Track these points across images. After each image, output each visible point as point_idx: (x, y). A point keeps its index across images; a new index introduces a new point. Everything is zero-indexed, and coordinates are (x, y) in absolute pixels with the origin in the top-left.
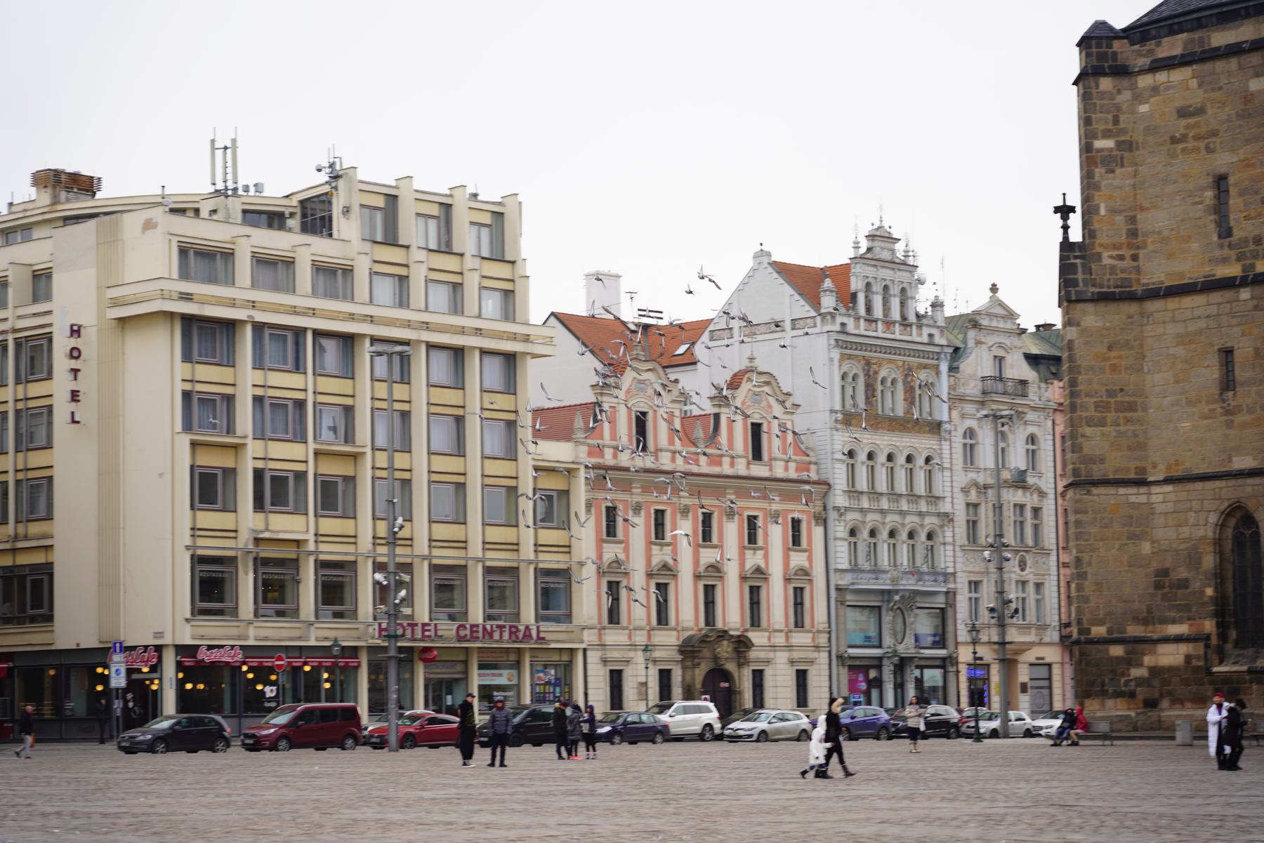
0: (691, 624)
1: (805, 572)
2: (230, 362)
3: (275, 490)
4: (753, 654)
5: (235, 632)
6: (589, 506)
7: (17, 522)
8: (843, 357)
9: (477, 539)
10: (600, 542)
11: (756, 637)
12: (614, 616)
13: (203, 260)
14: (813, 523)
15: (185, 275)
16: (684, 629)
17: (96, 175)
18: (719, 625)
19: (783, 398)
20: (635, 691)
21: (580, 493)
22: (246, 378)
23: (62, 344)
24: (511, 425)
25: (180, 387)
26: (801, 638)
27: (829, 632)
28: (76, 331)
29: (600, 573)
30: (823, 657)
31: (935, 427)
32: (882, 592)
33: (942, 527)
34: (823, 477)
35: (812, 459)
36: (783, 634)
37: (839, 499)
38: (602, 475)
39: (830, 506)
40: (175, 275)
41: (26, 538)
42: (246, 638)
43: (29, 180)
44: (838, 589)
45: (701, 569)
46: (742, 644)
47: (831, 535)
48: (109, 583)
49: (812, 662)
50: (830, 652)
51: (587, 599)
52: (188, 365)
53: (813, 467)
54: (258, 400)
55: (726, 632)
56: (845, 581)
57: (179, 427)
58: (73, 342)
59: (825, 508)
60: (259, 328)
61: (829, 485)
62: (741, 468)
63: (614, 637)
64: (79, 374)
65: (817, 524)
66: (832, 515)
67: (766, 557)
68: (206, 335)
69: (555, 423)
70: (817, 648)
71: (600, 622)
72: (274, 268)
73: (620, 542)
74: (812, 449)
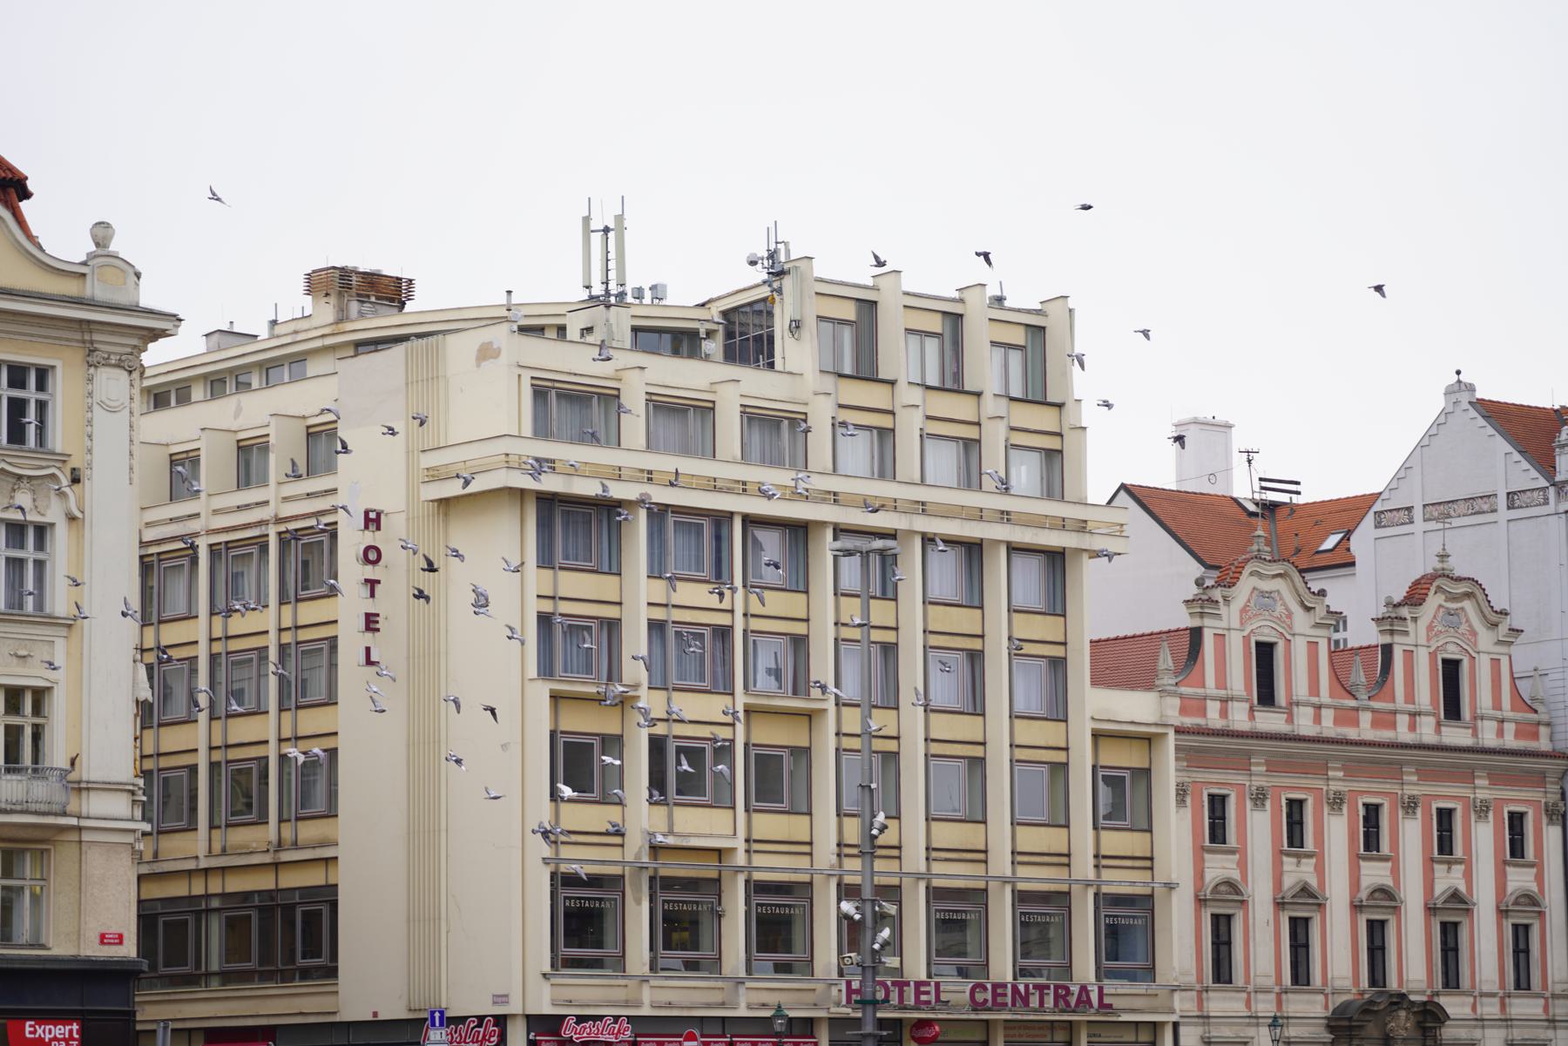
0: (1348, 983)
2: (614, 568)
3: (681, 771)
5: (620, 994)
6: (1182, 792)
7: (281, 821)
9: (1003, 847)
10: (1200, 852)
11: (1454, 1006)
12: (1222, 971)
13: (569, 406)
14: (1545, 820)
15: (542, 430)
17: (405, 275)
18: (1393, 984)
19: (1495, 617)
21: (1168, 770)
22: (638, 592)
23: (351, 540)
24: (1058, 665)
25: (534, 607)
28: (373, 520)
29: (1201, 902)
35: (1544, 717)
36: (1496, 1000)
38: (1206, 746)
40: (528, 430)
41: (295, 845)
42: (638, 1005)
43: (301, 285)
45: (1363, 895)
48: (424, 920)
51: (1180, 942)
52: (548, 573)
53: (1543, 730)
54: (656, 627)
55: (1403, 996)
57: (532, 671)
58: (369, 538)
60: (659, 513)
62: (1427, 731)
63: (1222, 1003)
64: (378, 588)
65: (1551, 822)
67: (1468, 875)
68: (575, 524)
69: (1122, 661)
71: (1200, 979)
72: (682, 417)
73: (1232, 852)
74: (1542, 702)
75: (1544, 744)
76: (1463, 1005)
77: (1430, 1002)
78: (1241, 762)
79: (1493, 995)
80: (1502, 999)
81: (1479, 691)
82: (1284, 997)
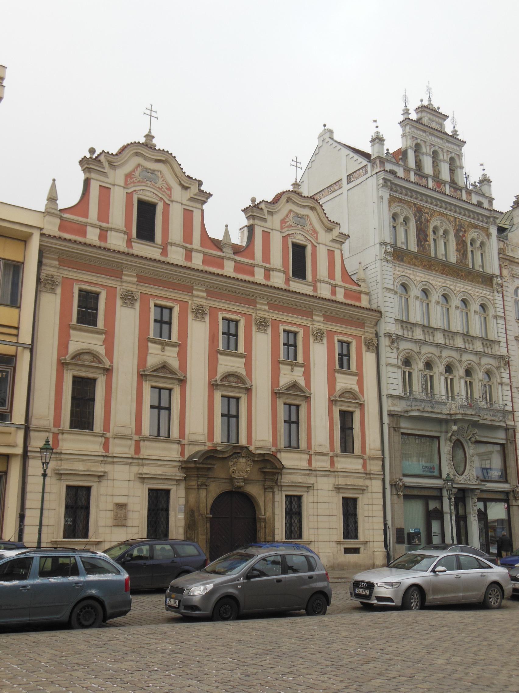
0: (203, 438)
4: (286, 479)
8: (392, 200)
11: (288, 459)
14: (364, 348)
16: (193, 443)
20: (110, 515)
26: (346, 463)
27: (383, 460)
30: (376, 486)
31: (487, 280)
32: (440, 421)
33: (498, 368)
34: (374, 307)
35: (365, 290)
36: (327, 458)
37: (388, 326)
39: (381, 334)
44: (391, 415)
46: (268, 467)
49: (363, 490)
50: (384, 480)
53: (363, 296)
56: (399, 407)
59: (377, 335)
61: (380, 312)
62: (278, 280)
65: (368, 349)
66: (384, 342)
67: (307, 375)
70: (368, 475)
74: (364, 281)
75: (364, 303)
76: (301, 459)
77: (274, 456)
78: (116, 272)
79: (325, 454)
80: (332, 458)
81: (319, 263)
82: (142, 443)
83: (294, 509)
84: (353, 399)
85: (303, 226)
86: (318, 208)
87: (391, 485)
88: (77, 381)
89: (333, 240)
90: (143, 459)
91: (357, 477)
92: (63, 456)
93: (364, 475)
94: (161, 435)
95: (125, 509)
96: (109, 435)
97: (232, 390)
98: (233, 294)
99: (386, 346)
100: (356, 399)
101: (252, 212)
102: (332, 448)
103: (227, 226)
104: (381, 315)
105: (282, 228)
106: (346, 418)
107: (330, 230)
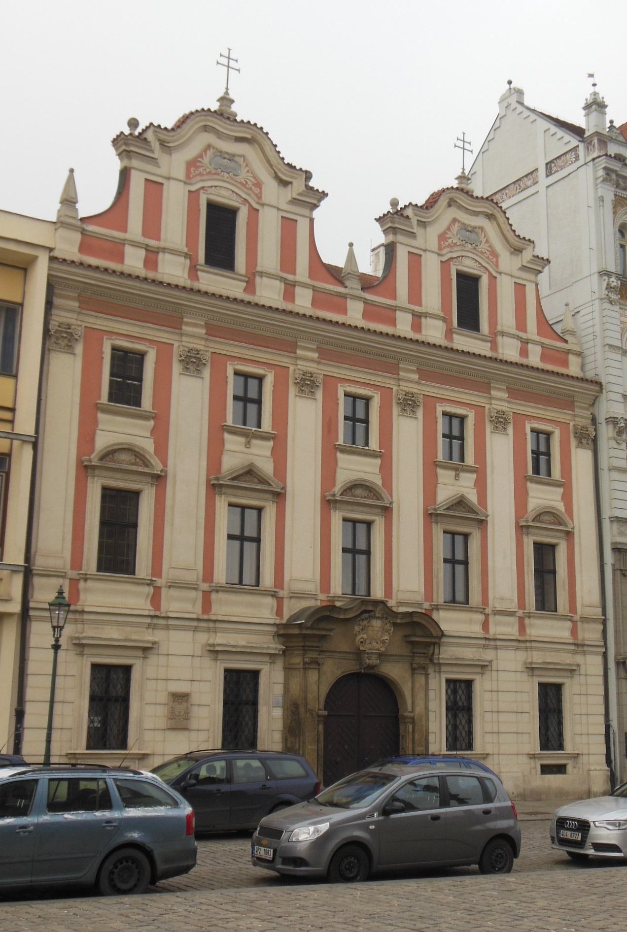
0: (313, 587)
1: (556, 520)
4: (447, 653)
8: (619, 203)
11: (450, 622)
14: (573, 442)
16: (297, 596)
20: (162, 711)
26: (544, 628)
27: (604, 622)
30: (592, 664)
34: (590, 375)
36: (514, 620)
39: (601, 419)
44: (617, 550)
46: (418, 634)
47: (604, 463)
49: (572, 671)
50: (605, 655)
53: (572, 358)
59: (594, 420)
61: (600, 384)
62: (434, 332)
63: (109, 598)
65: (580, 444)
66: (606, 432)
67: (481, 485)
70: (579, 647)
74: (573, 333)
75: (574, 369)
76: (471, 622)
77: (427, 616)
78: (172, 319)
80: (521, 619)
81: (500, 305)
82: (214, 596)
83: (460, 702)
84: (554, 523)
85: (475, 245)
86: (499, 215)
87: (618, 663)
88: (109, 495)
89: (524, 268)
90: (215, 621)
91: (564, 651)
92: (86, 617)
93: (573, 647)
94: (244, 582)
95: (187, 701)
96: (160, 582)
97: (359, 510)
98: (362, 354)
99: (609, 439)
100: (560, 524)
101: (392, 222)
102: (522, 604)
103: (351, 245)
104: (601, 389)
105: (440, 248)
106: (544, 554)
107: (518, 251)
